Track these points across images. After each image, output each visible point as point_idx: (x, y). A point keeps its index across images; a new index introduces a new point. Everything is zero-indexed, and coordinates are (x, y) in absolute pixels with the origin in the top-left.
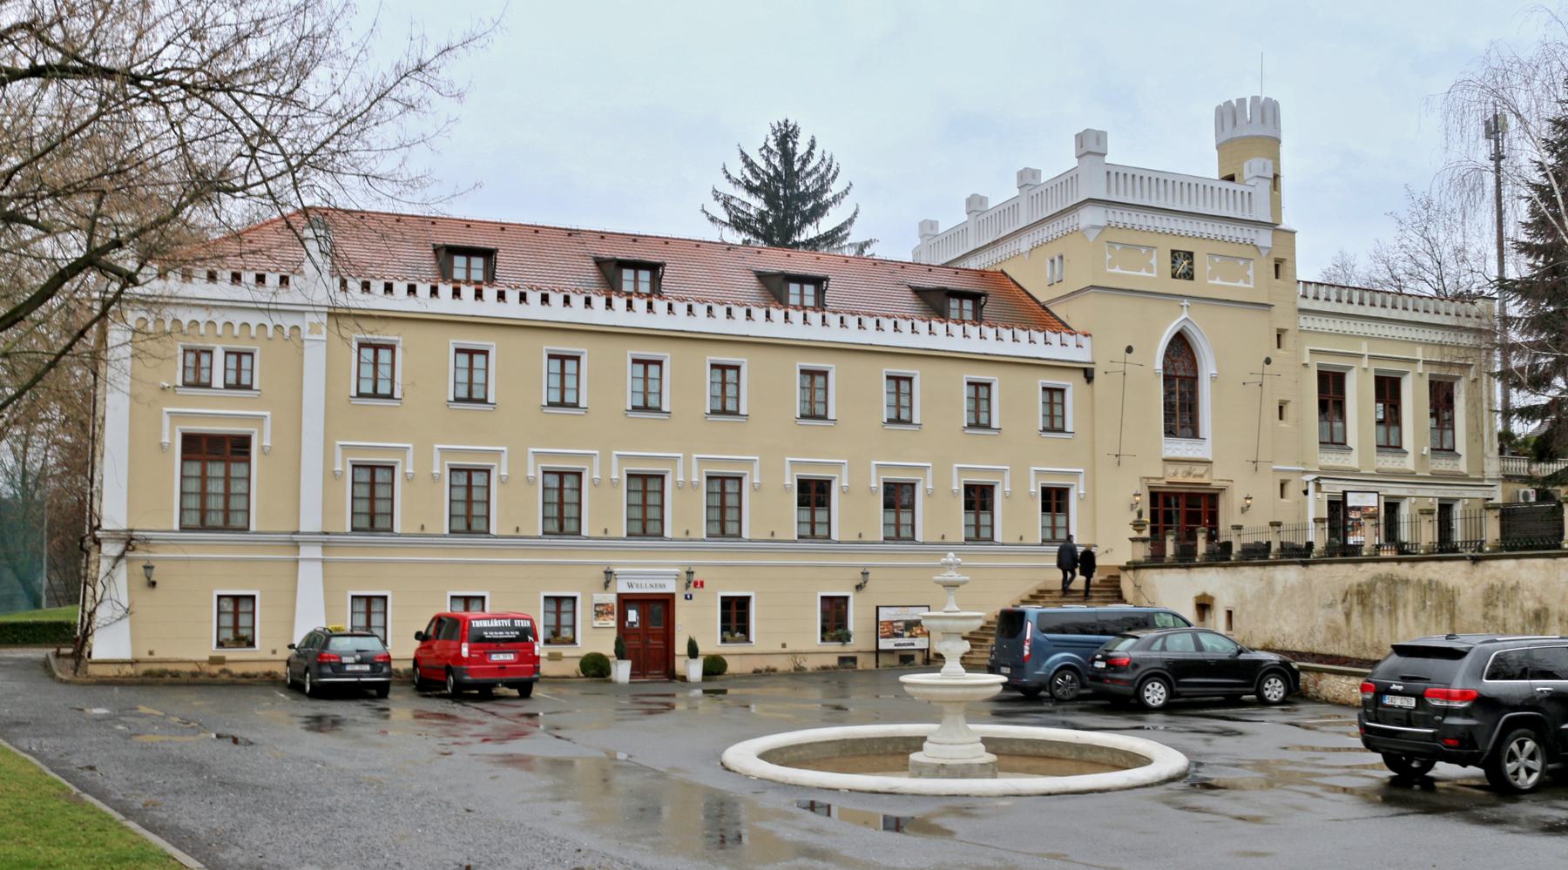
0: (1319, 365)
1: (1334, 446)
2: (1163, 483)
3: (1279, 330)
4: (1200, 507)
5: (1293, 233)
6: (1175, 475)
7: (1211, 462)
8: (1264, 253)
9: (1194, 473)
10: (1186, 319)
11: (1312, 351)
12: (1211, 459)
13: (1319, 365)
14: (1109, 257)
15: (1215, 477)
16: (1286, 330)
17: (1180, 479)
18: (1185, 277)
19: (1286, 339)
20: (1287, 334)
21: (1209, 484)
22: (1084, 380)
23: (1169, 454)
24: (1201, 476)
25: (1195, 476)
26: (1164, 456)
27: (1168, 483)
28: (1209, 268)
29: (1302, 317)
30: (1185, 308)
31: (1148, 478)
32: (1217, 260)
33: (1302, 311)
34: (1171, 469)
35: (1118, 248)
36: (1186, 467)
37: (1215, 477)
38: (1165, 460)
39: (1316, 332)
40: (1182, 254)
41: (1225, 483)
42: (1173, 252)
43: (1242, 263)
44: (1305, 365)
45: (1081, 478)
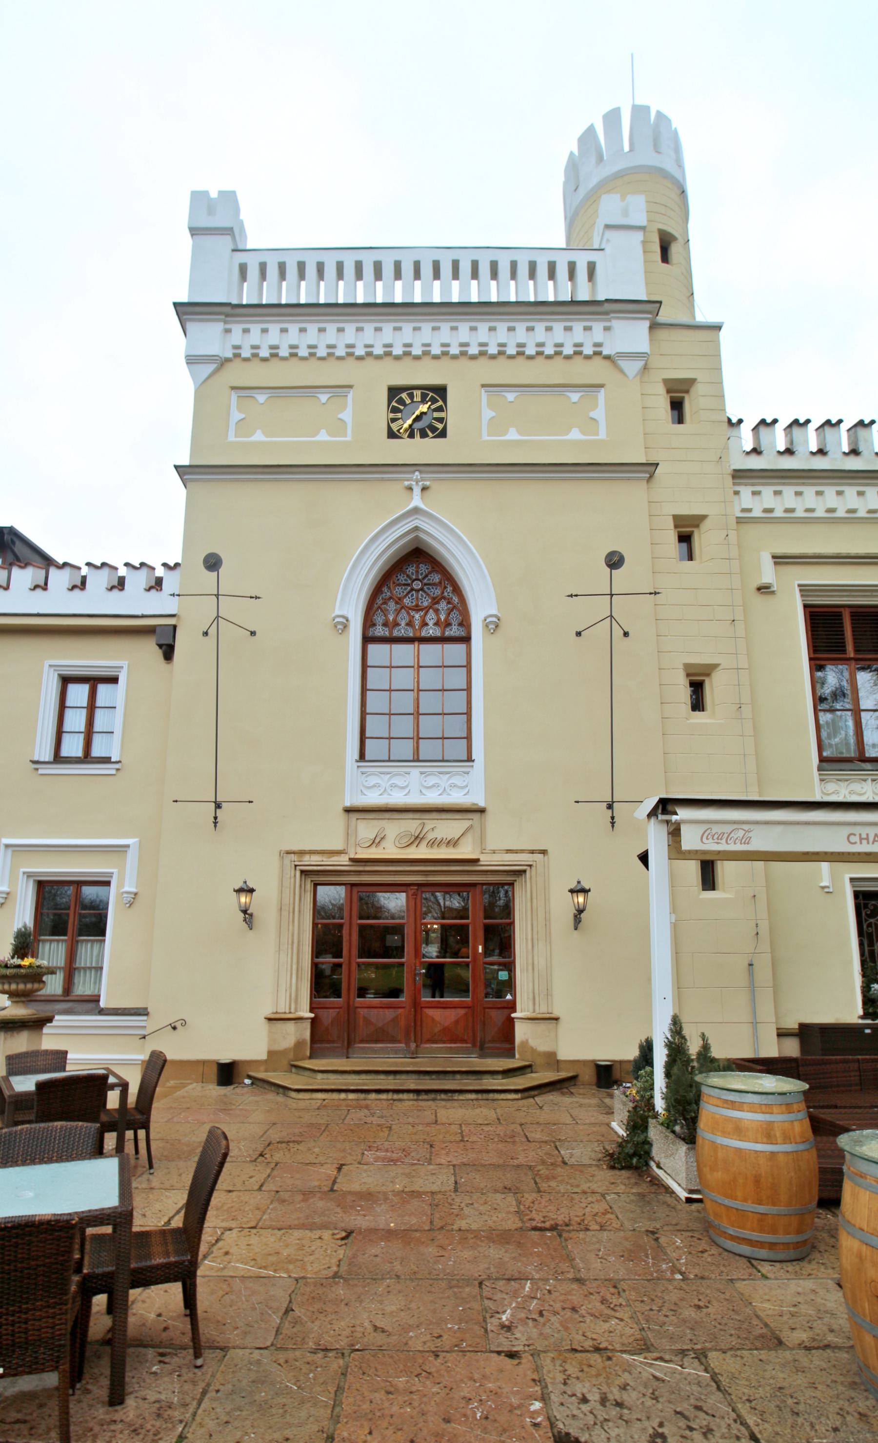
0: (804, 590)
1: (868, 766)
2: (344, 860)
3: (679, 521)
4: (467, 918)
5: (718, 328)
6: (376, 842)
7: (482, 811)
8: (632, 368)
9: (431, 836)
10: (416, 511)
11: (780, 560)
12: (482, 804)
13: (804, 590)
14: (236, 415)
15: (491, 845)
16: (703, 517)
17: (389, 850)
18: (424, 435)
19: (702, 540)
20: (705, 525)
21: (476, 861)
22: (159, 653)
23: (373, 799)
24: (453, 843)
25: (432, 844)
26: (348, 804)
27: (354, 861)
28: (487, 414)
29: (746, 492)
30: (417, 490)
31: (302, 853)
32: (511, 396)
33: (739, 475)
34: (366, 829)
35: (261, 398)
36: (411, 825)
37: (491, 845)
38: (348, 811)
39: (790, 519)
40: (417, 394)
41: (525, 858)
42: (394, 392)
43: (575, 397)
44: (764, 589)
45: (132, 857)
